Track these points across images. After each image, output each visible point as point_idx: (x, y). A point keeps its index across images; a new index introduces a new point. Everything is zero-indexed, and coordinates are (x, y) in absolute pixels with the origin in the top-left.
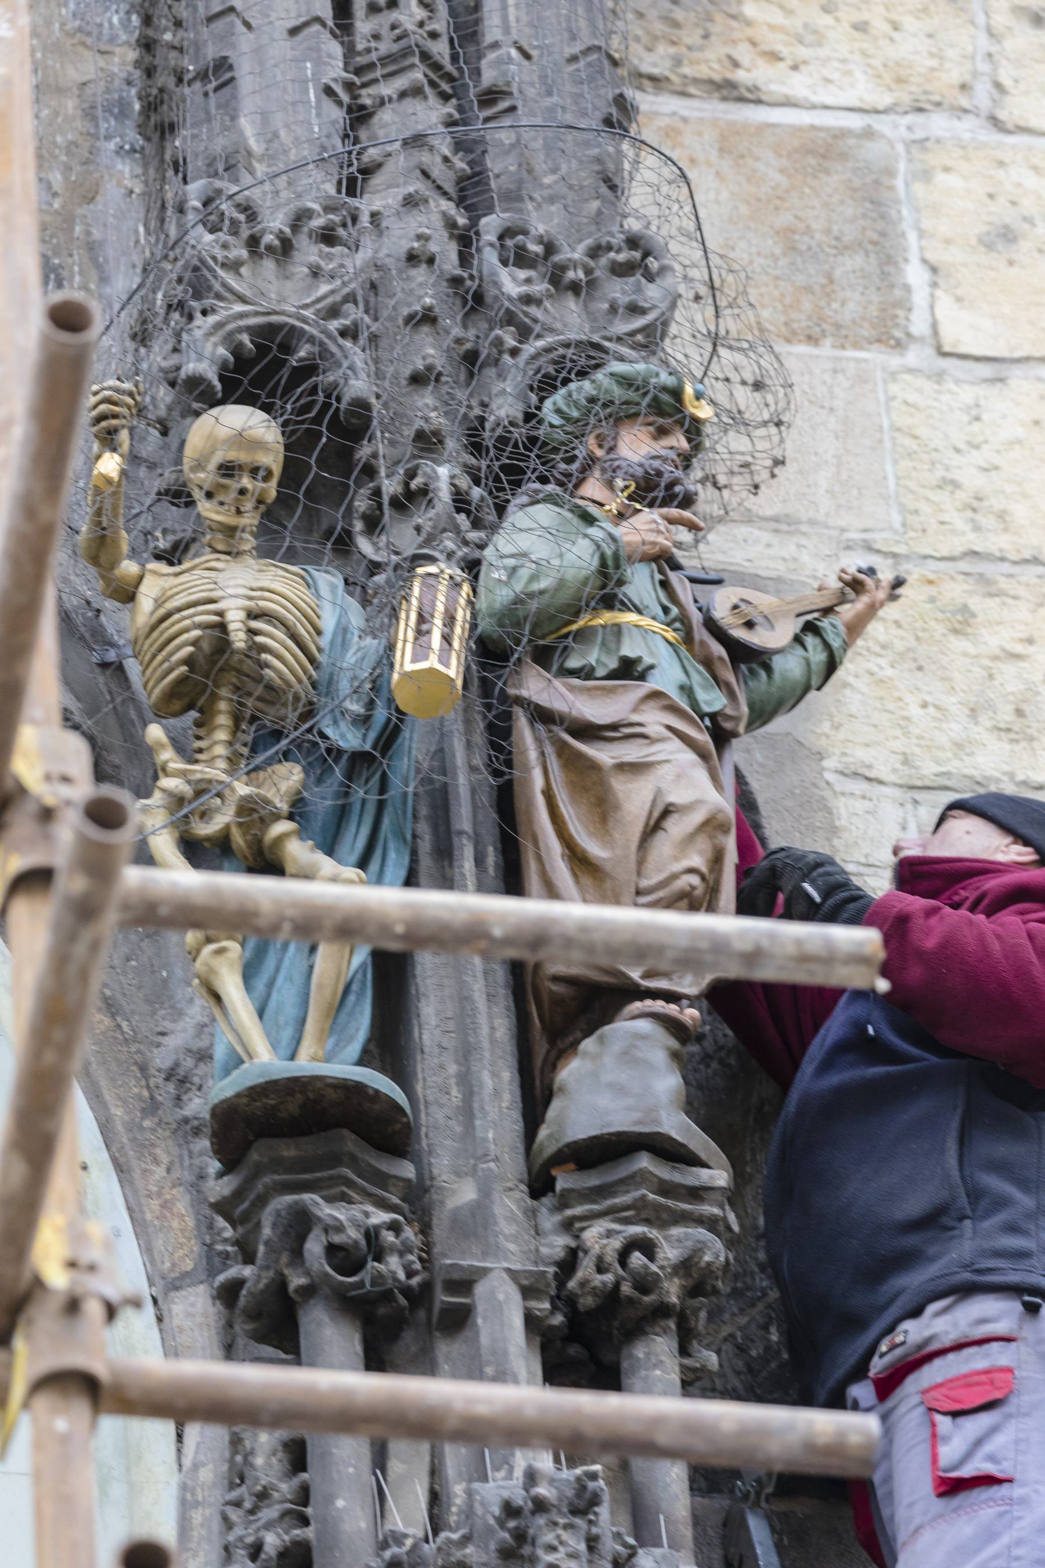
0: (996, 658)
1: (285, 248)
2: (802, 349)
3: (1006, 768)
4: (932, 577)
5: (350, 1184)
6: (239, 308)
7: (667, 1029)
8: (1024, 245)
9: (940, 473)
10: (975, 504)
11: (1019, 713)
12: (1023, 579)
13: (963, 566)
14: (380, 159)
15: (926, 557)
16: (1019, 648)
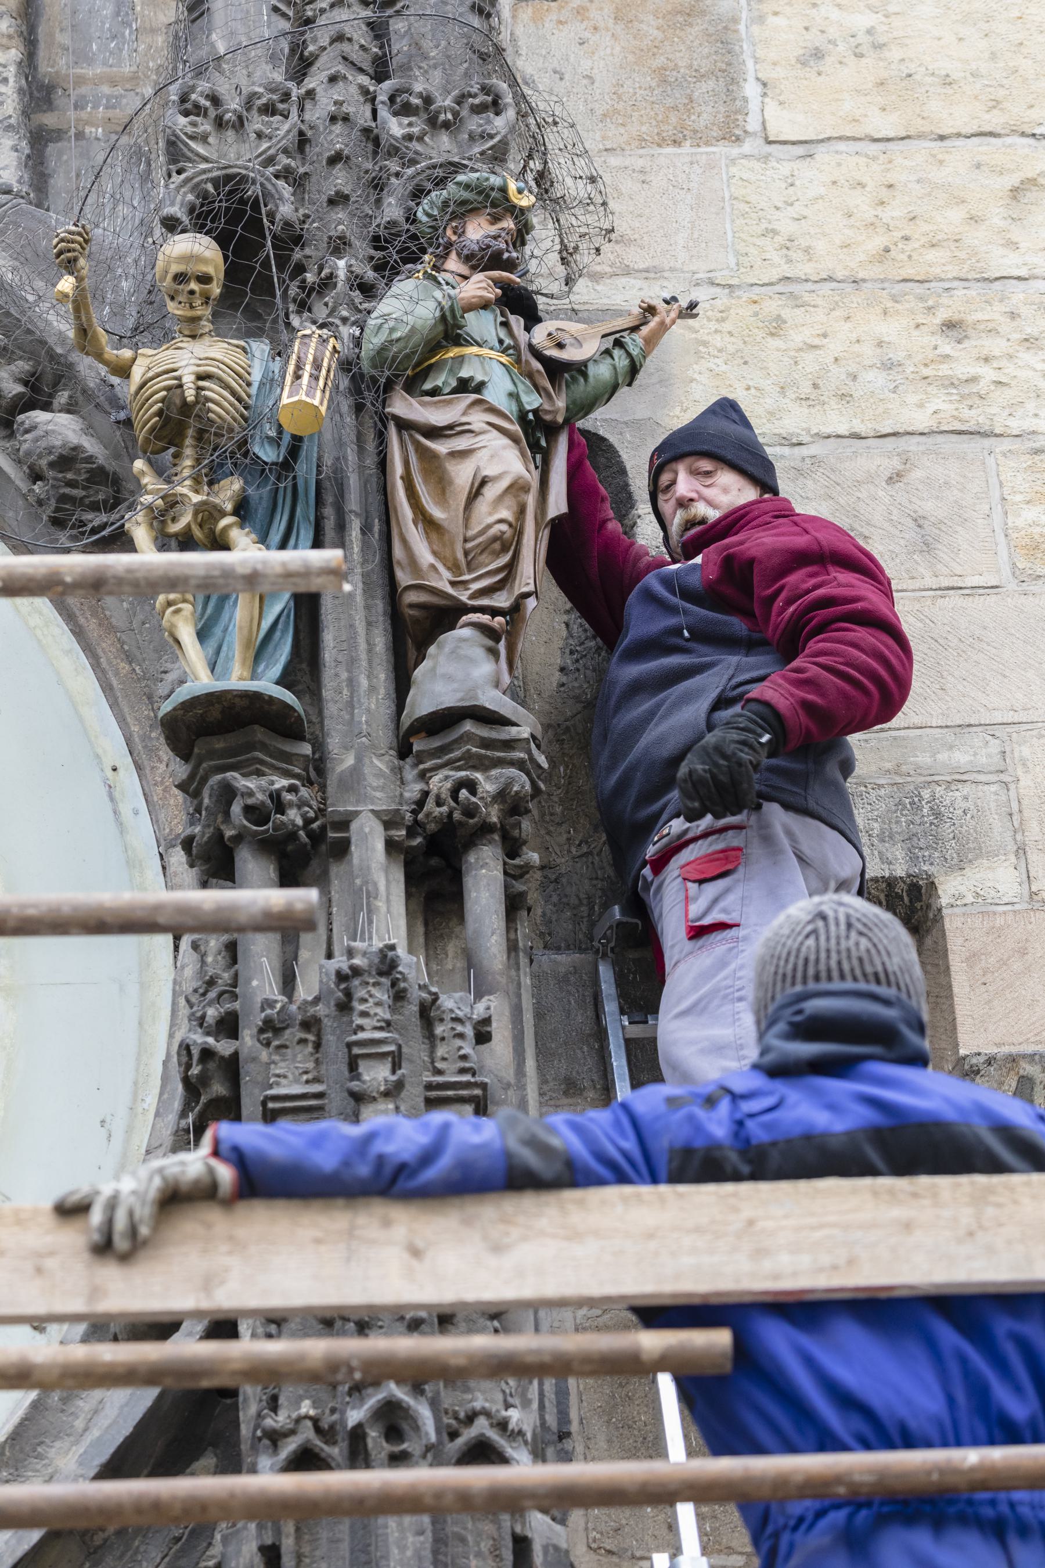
0: (801, 349)
2: (670, 150)
3: (804, 425)
4: (756, 298)
5: (262, 762)
6: (204, 166)
7: (483, 632)
8: (829, 60)
9: (764, 225)
10: (789, 244)
11: (815, 386)
12: (820, 293)
13: (779, 288)
15: (752, 285)
16: (817, 341)
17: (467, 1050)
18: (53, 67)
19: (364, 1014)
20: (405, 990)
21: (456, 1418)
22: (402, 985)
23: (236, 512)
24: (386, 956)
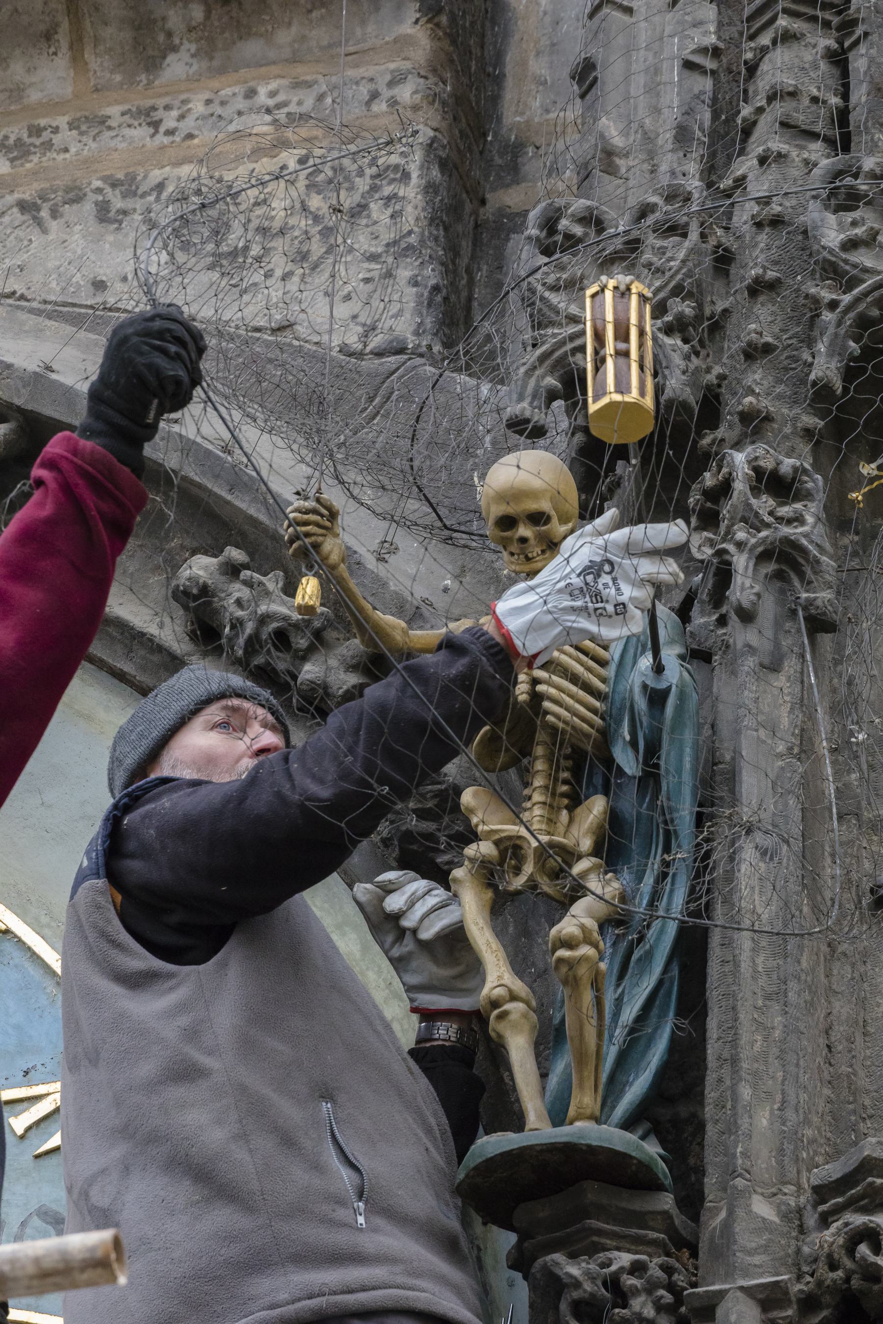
1: (634, 245)
5: (600, 1232)
14: (753, 118)
18: (522, 114)
23: (596, 851)
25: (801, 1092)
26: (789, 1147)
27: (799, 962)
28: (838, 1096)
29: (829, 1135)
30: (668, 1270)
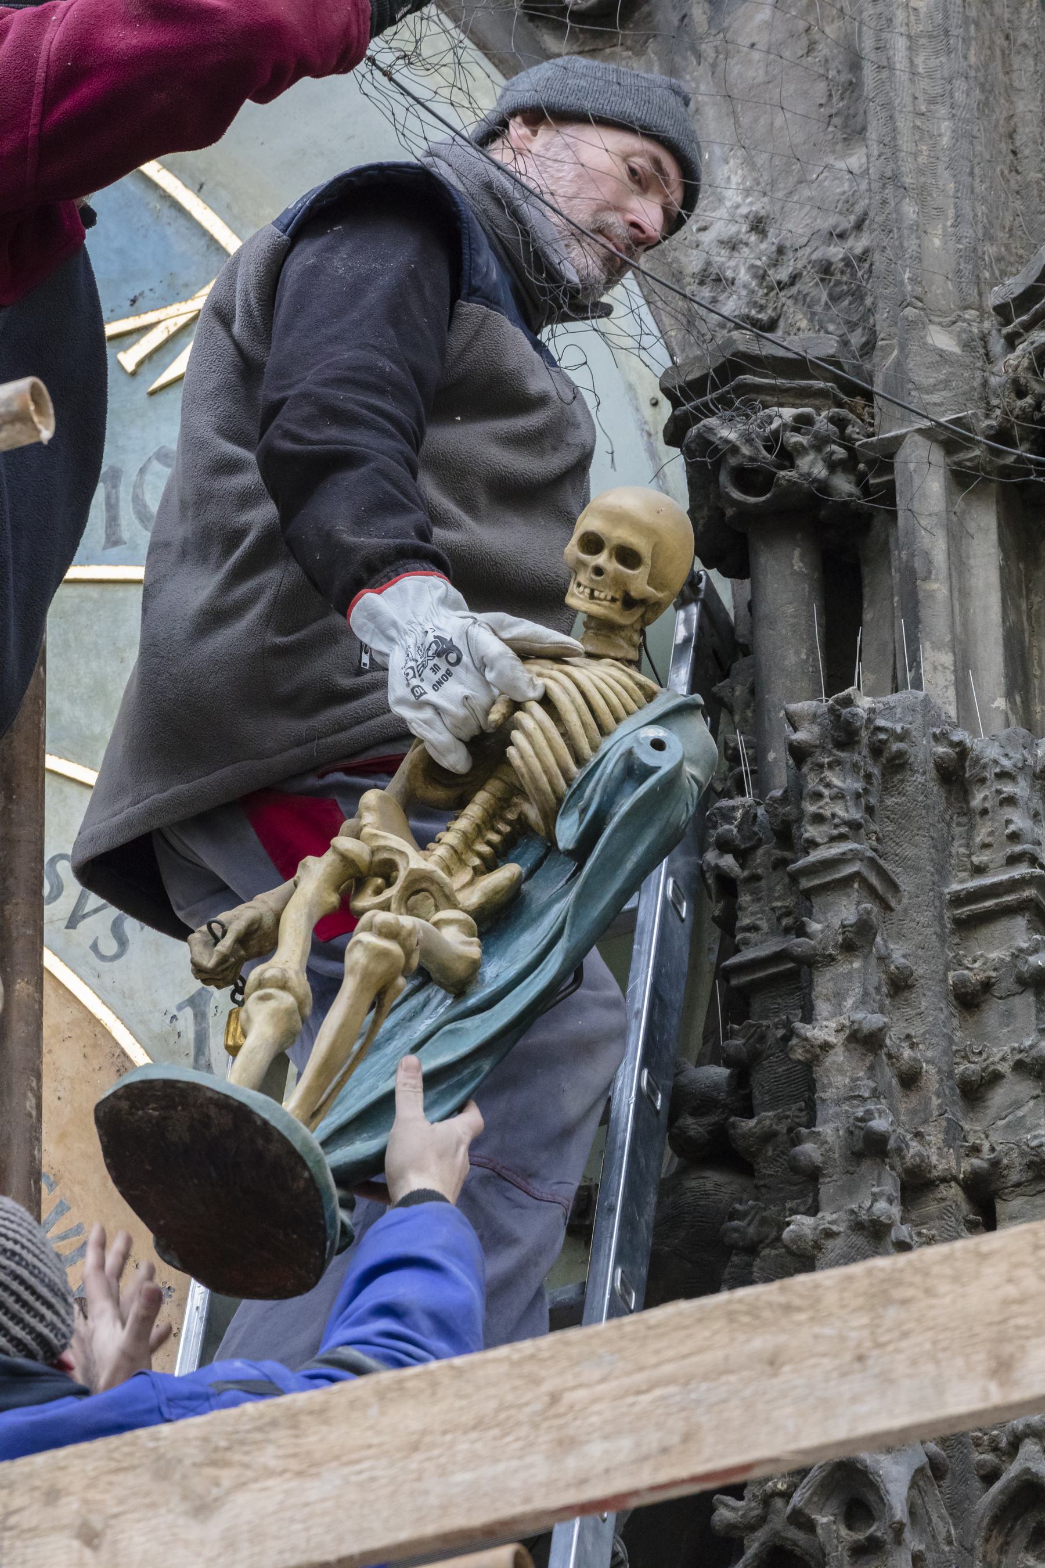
17: (1020, 821)
19: (818, 819)
20: (901, 754)
21: (995, 1449)
22: (895, 746)
24: (839, 716)
25: (978, 204)
26: (967, 268)
27: (965, 58)
28: (1028, 207)
29: (1021, 252)
30: (840, 423)
